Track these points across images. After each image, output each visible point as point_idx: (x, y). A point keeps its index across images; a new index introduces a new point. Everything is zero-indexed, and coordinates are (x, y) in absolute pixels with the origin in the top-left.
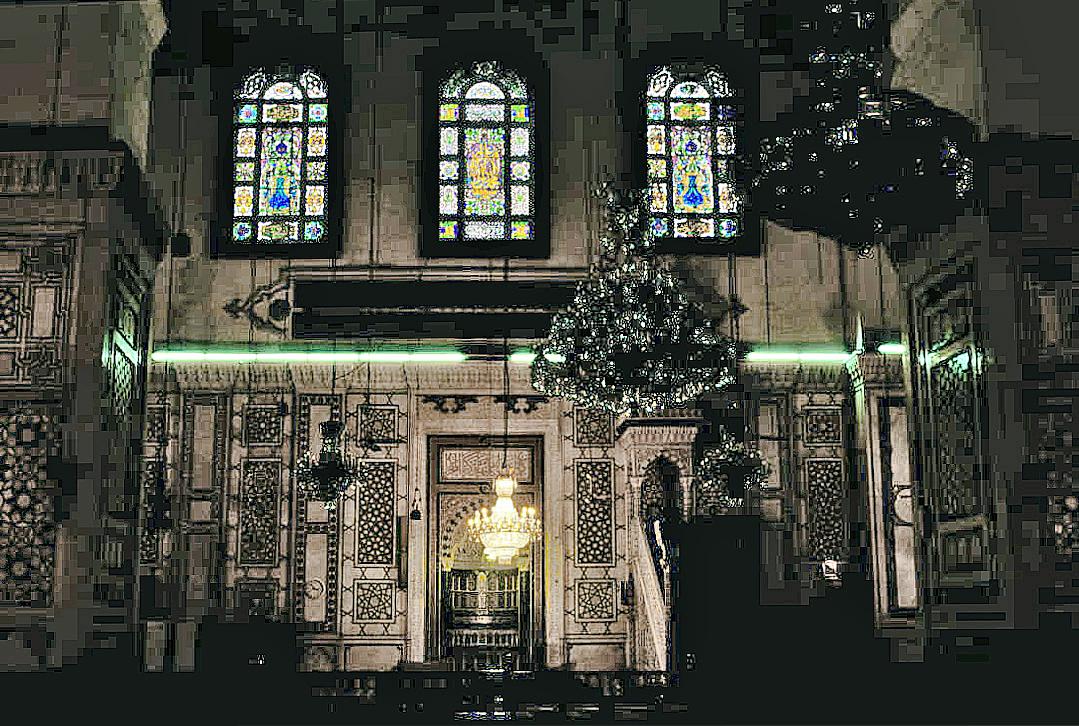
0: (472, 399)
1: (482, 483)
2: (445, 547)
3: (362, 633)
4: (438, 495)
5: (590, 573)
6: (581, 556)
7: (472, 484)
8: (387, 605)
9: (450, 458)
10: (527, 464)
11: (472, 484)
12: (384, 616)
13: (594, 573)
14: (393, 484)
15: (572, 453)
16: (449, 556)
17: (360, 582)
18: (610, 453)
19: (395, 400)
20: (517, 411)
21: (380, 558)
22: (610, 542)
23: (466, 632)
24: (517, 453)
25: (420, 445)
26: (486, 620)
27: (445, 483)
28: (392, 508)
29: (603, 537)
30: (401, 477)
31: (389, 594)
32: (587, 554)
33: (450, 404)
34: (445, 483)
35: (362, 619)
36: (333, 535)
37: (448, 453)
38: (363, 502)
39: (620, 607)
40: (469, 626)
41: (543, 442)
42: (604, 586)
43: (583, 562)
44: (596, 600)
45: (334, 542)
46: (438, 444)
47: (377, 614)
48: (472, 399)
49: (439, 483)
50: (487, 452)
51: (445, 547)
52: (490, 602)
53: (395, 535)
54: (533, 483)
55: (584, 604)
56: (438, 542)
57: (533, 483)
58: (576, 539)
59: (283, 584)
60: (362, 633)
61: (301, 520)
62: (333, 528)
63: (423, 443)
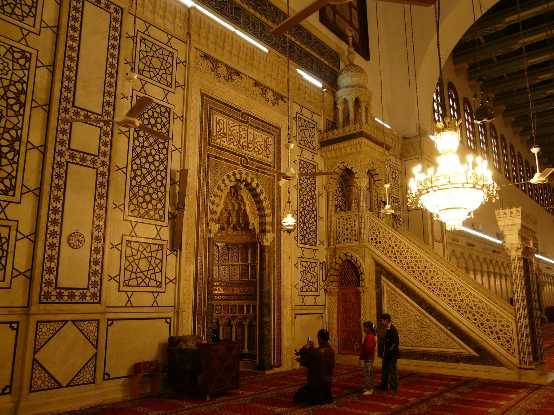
1: (241, 156)
3: (129, 304)
4: (208, 157)
7: (235, 154)
8: (157, 270)
11: (235, 154)
12: (153, 283)
13: (308, 254)
17: (130, 238)
20: (267, 100)
21: (152, 213)
22: (316, 228)
27: (215, 147)
31: (159, 256)
34: (215, 147)
35: (128, 286)
36: (103, 175)
37: (219, 118)
38: (137, 143)
39: (322, 284)
41: (280, 134)
42: (313, 265)
44: (309, 277)
45: (103, 187)
47: (147, 280)
53: (168, 190)
57: (274, 167)
59: (26, 228)
60: (129, 304)
61: (62, 143)
62: (103, 164)
63: (199, 98)
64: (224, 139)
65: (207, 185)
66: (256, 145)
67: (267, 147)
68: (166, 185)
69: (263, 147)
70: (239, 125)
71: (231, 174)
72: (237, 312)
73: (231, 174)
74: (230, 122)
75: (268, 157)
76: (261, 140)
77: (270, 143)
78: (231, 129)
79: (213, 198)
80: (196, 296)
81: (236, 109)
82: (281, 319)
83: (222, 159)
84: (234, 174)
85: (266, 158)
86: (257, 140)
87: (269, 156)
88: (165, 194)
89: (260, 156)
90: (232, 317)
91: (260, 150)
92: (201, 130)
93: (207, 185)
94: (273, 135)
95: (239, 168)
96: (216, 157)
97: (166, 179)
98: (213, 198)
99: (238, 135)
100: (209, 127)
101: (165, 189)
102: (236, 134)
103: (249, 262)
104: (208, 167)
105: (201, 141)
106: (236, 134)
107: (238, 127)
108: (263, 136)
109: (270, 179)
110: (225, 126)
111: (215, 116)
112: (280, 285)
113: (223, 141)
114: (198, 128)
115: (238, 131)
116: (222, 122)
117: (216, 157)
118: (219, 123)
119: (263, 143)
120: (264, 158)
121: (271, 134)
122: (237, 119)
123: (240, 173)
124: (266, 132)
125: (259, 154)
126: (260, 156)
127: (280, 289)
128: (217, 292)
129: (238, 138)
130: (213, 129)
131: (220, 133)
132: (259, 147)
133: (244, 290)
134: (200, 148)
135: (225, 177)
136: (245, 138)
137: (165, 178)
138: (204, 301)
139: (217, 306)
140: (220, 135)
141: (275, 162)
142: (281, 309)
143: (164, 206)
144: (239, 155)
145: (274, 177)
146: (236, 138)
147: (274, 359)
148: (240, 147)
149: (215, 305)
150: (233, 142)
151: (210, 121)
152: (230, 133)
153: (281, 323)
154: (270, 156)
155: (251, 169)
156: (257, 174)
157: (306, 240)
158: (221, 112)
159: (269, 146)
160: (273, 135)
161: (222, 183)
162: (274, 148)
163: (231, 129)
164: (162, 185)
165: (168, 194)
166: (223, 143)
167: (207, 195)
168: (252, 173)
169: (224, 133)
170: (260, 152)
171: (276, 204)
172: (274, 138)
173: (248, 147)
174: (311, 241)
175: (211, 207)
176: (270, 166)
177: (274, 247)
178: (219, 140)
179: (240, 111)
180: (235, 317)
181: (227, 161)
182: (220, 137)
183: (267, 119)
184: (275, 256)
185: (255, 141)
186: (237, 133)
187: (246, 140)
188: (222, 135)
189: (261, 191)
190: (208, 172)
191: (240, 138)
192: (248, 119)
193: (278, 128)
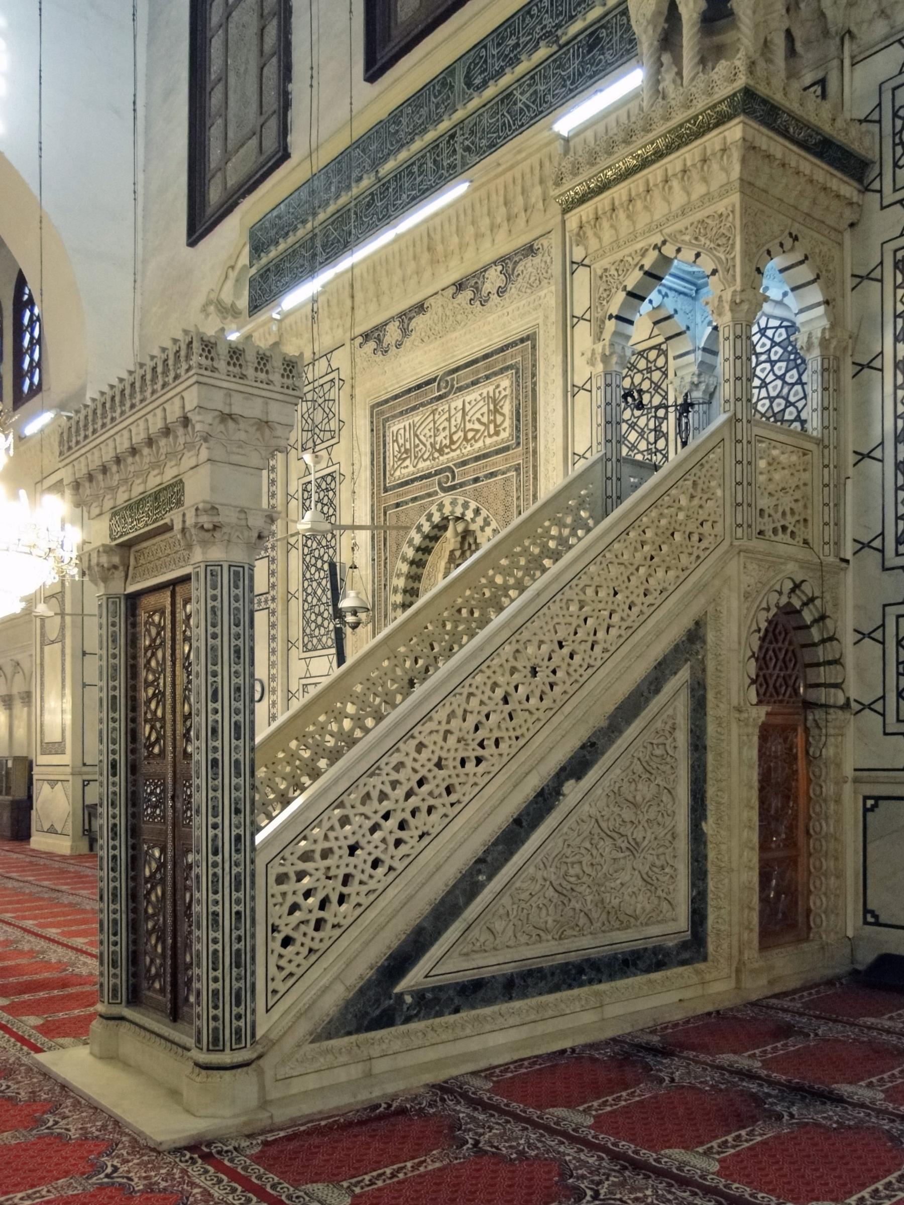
48: (420, 308)
74: (416, 419)
77: (503, 393)
85: (495, 438)
89: (480, 444)
120: (488, 441)
126: (480, 444)
132: (477, 426)
136: (444, 429)
145: (517, 469)
152: (417, 442)
155: (461, 485)
160: (510, 367)
168: (465, 492)
173: (452, 442)
183: (497, 340)
185: (467, 418)
189: (485, 520)
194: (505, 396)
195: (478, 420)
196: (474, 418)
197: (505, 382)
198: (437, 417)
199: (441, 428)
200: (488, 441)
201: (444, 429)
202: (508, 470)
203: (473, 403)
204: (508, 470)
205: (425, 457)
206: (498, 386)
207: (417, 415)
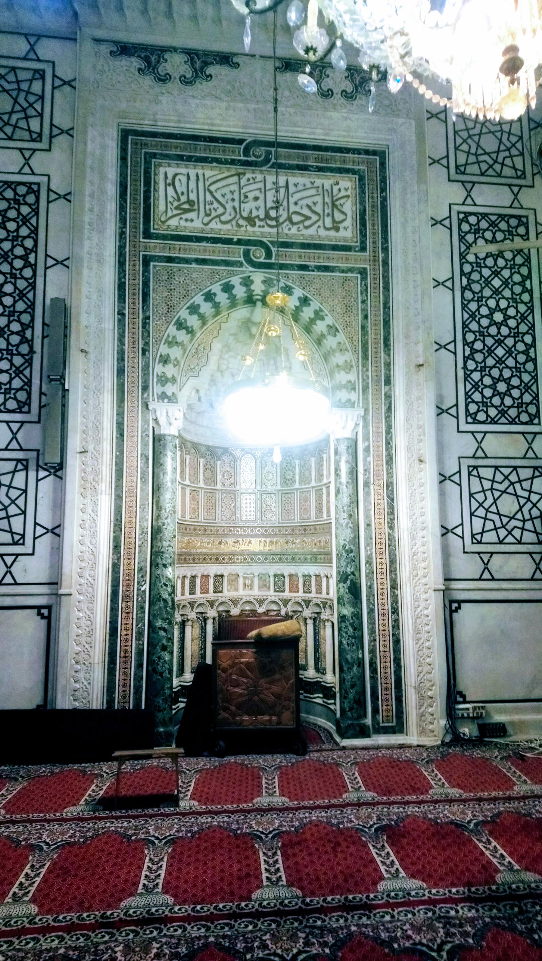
0: (226, 59)
1: (248, 243)
2: (163, 380)
5: (494, 445)
6: (473, 408)
9: (174, 180)
10: (349, 207)
11: (228, 241)
14: (35, 231)
15: (445, 195)
16: (172, 399)
18: (528, 198)
19: (48, 49)
23: (213, 569)
24: (327, 184)
25: (102, 148)
26: (256, 545)
27: (164, 237)
28: (33, 286)
29: (518, 370)
30: (56, 216)
32: (485, 404)
33: (175, 65)
34: (164, 237)
37: (171, 171)
40: (230, 558)
43: (476, 422)
46: (142, 153)
49: (147, 235)
50: (259, 177)
51: (163, 380)
52: (262, 510)
53: (37, 347)
54: (363, 249)
55: (481, 512)
56: (146, 367)
57: (363, 249)
58: (461, 373)
64: (190, 215)
65: (145, 325)
66: (293, 208)
67: (334, 205)
68: (32, 340)
69: (318, 208)
70: (238, 175)
71: (216, 288)
72: (313, 589)
73: (216, 288)
74: (209, 173)
75: (337, 229)
76: (313, 192)
78: (213, 188)
79: (164, 349)
80: (119, 559)
81: (226, 141)
82: (395, 611)
83: (187, 261)
84: (228, 288)
85: (332, 233)
86: (297, 196)
87: (341, 226)
88: (31, 358)
89: (312, 231)
90: (304, 601)
91: (309, 218)
92: (122, 208)
93: (145, 325)
94: (354, 172)
95: (244, 272)
96: (170, 260)
97: (33, 328)
98: (164, 349)
99: (236, 196)
100: (147, 198)
101: (31, 347)
102: (229, 196)
103: (325, 481)
104: (146, 284)
105: (122, 234)
106: (229, 196)
107: (235, 179)
108: (318, 182)
109: (346, 279)
110: (192, 185)
111: (162, 170)
112: (391, 528)
113: (186, 220)
114: (112, 207)
115: (235, 187)
116: (184, 179)
117: (170, 260)
118: (173, 184)
119: (319, 199)
120: (322, 233)
121: (348, 171)
122: (233, 162)
123: (247, 282)
124: (331, 170)
125: (306, 228)
126: (312, 231)
127: (391, 538)
128: (273, 547)
129: (236, 204)
130: (156, 199)
131: (176, 204)
133: (320, 541)
134: (122, 247)
135: (199, 299)
136: (256, 199)
137: (31, 325)
138: (140, 570)
139: (275, 576)
140: (177, 208)
141: (363, 235)
142: (394, 587)
143: (29, 383)
144: (239, 242)
145: (363, 272)
146: (229, 206)
147: (375, 711)
148: (241, 222)
149: (272, 574)
150: (219, 216)
151: (148, 183)
152: (209, 198)
153: (396, 621)
154: (346, 224)
156: (302, 277)
157: (493, 412)
158: (181, 158)
159: (342, 201)
160: (354, 172)
161: (191, 313)
162: (362, 202)
163: (213, 188)
164: (24, 340)
165: (37, 359)
166: (189, 224)
167: (147, 344)
168: (287, 276)
169: (190, 202)
170: (307, 223)
171: (371, 338)
172: (361, 179)
174: (513, 412)
175: (159, 369)
176: (347, 248)
177: (366, 438)
178: (177, 218)
179: (240, 142)
180: (310, 601)
181: (203, 262)
182: (175, 212)
184: (370, 459)
185: (292, 200)
186: (232, 192)
187: (261, 203)
188: (186, 206)
189: (316, 313)
190: (146, 296)
191: (240, 202)
192: (270, 153)
193: (374, 153)
194: (348, 196)
195: (308, 206)
196: (304, 202)
197: (346, 184)
198: (243, 181)
199: (251, 196)
200: (322, 233)
201: (256, 199)
202: (351, 270)
203: (300, 187)
204: (351, 270)
205: (223, 218)
206: (338, 184)
207: (212, 169)
